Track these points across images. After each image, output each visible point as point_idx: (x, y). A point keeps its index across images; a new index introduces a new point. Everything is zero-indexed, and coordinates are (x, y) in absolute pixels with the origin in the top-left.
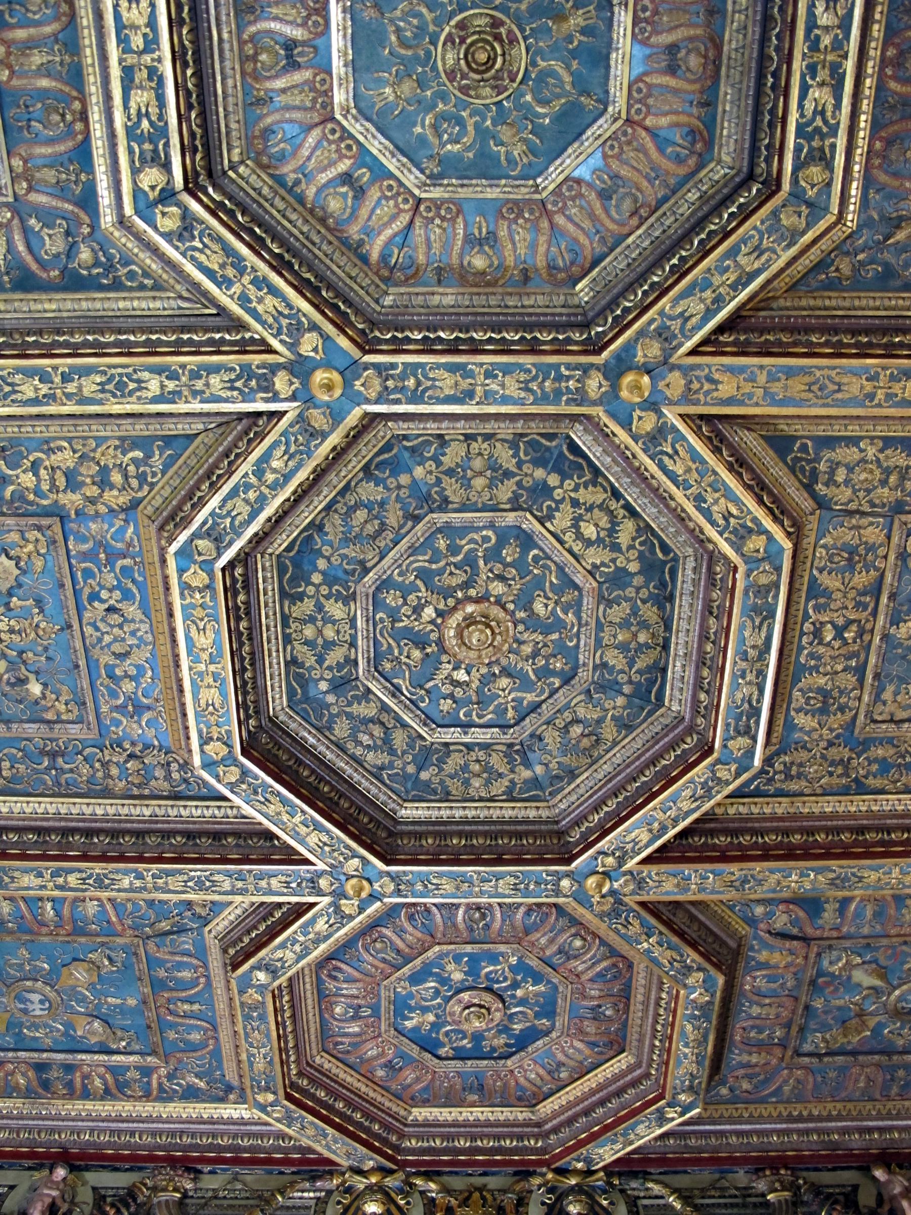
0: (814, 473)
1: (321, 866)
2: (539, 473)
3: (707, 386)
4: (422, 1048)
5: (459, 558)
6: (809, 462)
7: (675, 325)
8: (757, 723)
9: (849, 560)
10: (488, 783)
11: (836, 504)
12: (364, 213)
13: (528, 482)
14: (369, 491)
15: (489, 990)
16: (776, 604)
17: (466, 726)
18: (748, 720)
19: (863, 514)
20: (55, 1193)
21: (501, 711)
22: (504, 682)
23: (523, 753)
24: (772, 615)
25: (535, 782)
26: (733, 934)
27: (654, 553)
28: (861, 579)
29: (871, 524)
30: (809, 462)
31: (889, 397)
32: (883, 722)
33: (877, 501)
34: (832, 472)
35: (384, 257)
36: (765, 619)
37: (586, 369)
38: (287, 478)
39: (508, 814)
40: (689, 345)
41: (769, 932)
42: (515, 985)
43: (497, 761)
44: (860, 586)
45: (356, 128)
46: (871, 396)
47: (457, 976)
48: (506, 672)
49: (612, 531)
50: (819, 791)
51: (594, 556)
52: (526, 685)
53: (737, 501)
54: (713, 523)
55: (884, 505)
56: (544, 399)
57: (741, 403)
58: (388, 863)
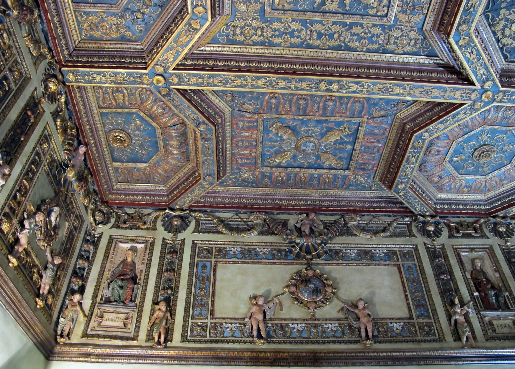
0: (422, 43)
7: (468, 112)
11: (415, 31)
16: (462, 15)
24: (465, 10)
30: (424, 48)
31: (405, 88)
33: (399, 31)
36: (468, 10)
37: (501, 101)
46: (411, 89)
53: (465, 57)
54: (477, 50)
55: (396, 29)
57: (454, 88)
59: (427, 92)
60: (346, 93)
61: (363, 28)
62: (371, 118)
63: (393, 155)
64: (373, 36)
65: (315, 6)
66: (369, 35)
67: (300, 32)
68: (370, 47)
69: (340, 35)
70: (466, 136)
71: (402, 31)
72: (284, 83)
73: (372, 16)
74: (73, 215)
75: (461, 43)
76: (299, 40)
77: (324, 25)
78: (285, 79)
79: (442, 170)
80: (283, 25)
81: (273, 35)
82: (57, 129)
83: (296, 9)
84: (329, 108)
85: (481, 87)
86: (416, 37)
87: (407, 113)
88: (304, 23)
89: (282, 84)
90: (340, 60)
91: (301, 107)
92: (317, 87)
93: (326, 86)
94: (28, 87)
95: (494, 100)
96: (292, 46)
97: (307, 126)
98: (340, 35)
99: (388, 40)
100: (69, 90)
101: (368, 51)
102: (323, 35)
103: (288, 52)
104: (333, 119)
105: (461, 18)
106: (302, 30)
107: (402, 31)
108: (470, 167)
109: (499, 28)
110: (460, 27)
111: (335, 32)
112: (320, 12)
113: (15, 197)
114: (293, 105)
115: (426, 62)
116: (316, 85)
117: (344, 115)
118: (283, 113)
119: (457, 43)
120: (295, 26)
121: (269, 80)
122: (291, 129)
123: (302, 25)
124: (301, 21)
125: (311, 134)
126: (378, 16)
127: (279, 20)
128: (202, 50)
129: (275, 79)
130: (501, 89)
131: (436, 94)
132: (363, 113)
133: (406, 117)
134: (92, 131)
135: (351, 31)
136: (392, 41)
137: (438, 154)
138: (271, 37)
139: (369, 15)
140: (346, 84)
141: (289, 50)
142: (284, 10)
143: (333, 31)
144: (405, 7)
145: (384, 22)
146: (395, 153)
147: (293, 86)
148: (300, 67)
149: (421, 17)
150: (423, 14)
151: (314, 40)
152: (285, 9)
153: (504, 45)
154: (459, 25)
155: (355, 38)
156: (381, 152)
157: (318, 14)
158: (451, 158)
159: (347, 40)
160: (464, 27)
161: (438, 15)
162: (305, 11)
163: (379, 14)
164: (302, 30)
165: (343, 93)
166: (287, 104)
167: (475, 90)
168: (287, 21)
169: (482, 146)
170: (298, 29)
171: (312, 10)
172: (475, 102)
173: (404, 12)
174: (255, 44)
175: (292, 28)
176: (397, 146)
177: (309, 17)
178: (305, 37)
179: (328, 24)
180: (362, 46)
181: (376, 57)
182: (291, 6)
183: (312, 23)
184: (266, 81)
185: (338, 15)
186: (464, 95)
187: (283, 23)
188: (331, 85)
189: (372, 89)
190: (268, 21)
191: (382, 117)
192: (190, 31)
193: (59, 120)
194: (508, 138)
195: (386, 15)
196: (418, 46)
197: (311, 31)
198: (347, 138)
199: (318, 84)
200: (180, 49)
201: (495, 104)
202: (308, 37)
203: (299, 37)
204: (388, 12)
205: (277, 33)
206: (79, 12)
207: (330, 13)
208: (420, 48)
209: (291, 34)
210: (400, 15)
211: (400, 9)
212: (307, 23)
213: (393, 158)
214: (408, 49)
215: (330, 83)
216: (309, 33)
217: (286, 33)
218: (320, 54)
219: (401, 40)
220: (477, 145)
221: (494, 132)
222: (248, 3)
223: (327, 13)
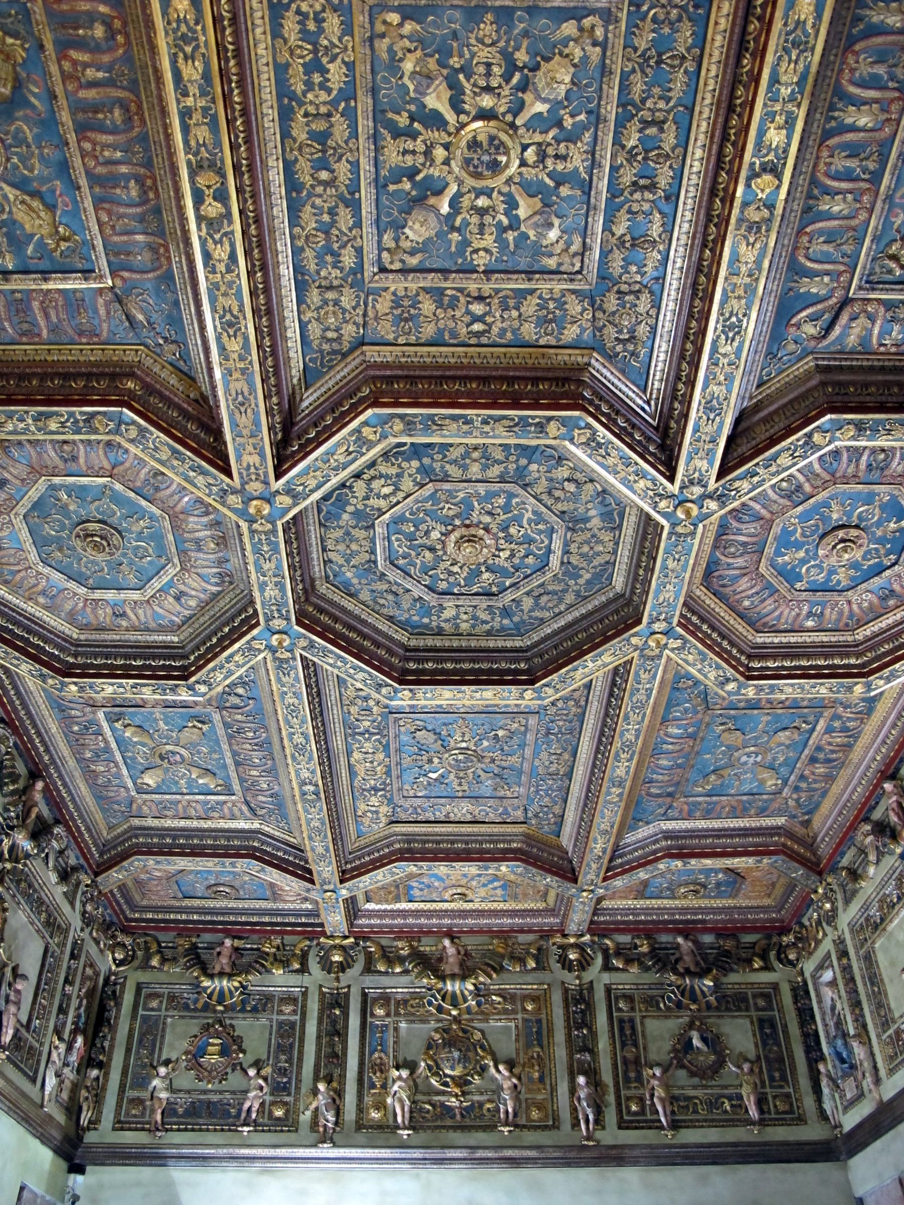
0: (334, 352)
1: (636, 654)
2: (345, 516)
3: (252, 470)
4: (877, 574)
5: (413, 553)
6: (323, 357)
8: (533, 418)
9: (406, 320)
10: (600, 542)
12: (193, 593)
13: (353, 522)
14: (365, 596)
15: (823, 536)
17: (549, 551)
18: (530, 425)
19: (365, 315)
20: (894, 798)
21: (540, 532)
22: (512, 531)
23: (577, 521)
25: (607, 516)
26: (808, 375)
27: (404, 453)
28: (427, 306)
29: (374, 307)
30: (323, 357)
32: (582, 261)
34: (329, 340)
35: (217, 584)
37: (252, 532)
38: (340, 657)
39: (630, 532)
40: (227, 480)
41: (824, 337)
42: (825, 519)
43: (580, 538)
44: (433, 307)
45: (150, 592)
46: (243, 371)
47: (802, 554)
48: (505, 529)
49: (387, 477)
50: (653, 312)
51: (407, 484)
52: (518, 520)
56: (276, 550)
58: (639, 622)
59: (242, 404)
60: (200, 237)
61: (350, 230)
62: (116, 295)
63: (34, 375)
64: (336, 255)
65: (390, 115)
66: (336, 246)
67: (323, 86)
68: (309, 253)
69: (326, 184)
70: (132, 495)
71: (354, 308)
72: (196, 77)
73: (379, 242)
75: (367, 431)
76: (299, 88)
77: (346, 142)
78: (206, 76)
79: (23, 480)
81: (305, 16)
83: (377, 69)
84: (118, 191)
85: (277, 492)
86: (346, 337)
87: (156, 369)
88: (348, 94)
89: (192, 72)
90: (268, 195)
91: (100, 116)
92: (201, 167)
93: (209, 187)
95: (251, 521)
96: (281, 70)
97: (38, 138)
98: (326, 184)
99: (330, 288)
101: (297, 252)
102: (323, 144)
103: (264, 61)
104: (88, 203)
105: (415, 416)
106: (329, 91)
107: (354, 308)
108: (52, 528)
109: (383, 468)
110: (397, 420)
111: (333, 171)
112: (375, 128)
114: (100, 90)
115: (294, 372)
116: (206, 164)
117: (108, 231)
118: (67, 65)
119: (366, 423)
120: (336, 73)
121: (195, 32)
122: (13, 93)
123: (340, 89)
124: (352, 84)
125: (16, 154)
126: (379, 255)
127: (348, 29)
129: (203, 50)
130: (279, 524)
131: (243, 420)
132: (126, 274)
133: (148, 372)
135: (341, 205)
136: (330, 295)
137: (66, 461)
138: (298, 12)
139: (380, 236)
140: (226, 234)
141: (267, 64)
142: (371, 39)
143: (335, 166)
144: (406, 303)
145: (370, 269)
146: (43, 377)
147: (190, 101)
148: (238, 107)
149: (391, 337)
150: (396, 339)
151: (307, 125)
152: (377, 43)
153: (351, 487)
154: (402, 417)
155: (326, 218)
156: (24, 339)
157: (371, 124)
158: (62, 486)
159: (318, 201)
160: (398, 426)
161: (401, 367)
162: (374, 91)
163: (385, 255)
164: (329, 91)
165: (199, 229)
166: (100, 75)
167: (266, 483)
168: (346, 49)
169: (115, 529)
170: (328, 80)
171: (379, 108)
172: (241, 491)
173: (397, 302)
175: (331, 66)
176: (66, 376)
177: (364, 103)
178: (311, 102)
179: (351, 150)
180: (307, 237)
181: (286, 272)
182: (385, 56)
183: (350, 115)
184: (192, 23)
185: (373, 170)
186: (252, 470)
187: (340, 40)
188: (215, 199)
189: (225, 295)
191: (128, 317)
194: (150, 563)
195: (383, 270)
196: (326, 347)
197: (329, 115)
198: (35, 250)
199: (212, 165)
201: (244, 526)
202: (311, 109)
203: (309, 86)
204: (392, 271)
205: (312, 26)
207: (376, 150)
208: (321, 351)
209: (315, 66)
210: (388, 296)
211: (401, 293)
212: (347, 100)
213: (29, 377)
214: (315, 330)
215: (221, 196)
216: (323, 110)
217: (315, 51)
218: (272, 145)
219: (334, 313)
220: (114, 521)
221: (157, 538)
223: (375, 144)
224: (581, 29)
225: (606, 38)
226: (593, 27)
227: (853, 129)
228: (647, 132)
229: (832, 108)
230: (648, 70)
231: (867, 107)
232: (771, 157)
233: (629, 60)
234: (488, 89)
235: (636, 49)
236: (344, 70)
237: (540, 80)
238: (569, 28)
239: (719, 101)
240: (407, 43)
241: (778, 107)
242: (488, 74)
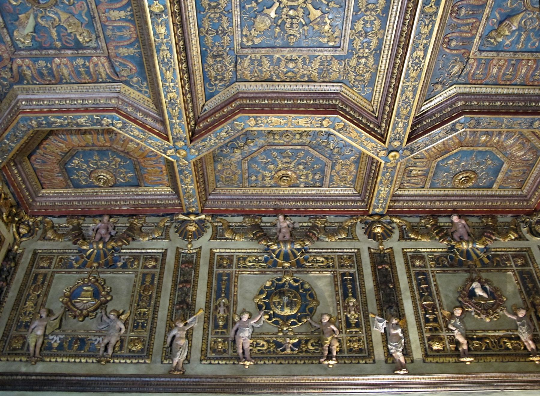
67: (367, 22)
74: (508, 260)
80: (356, 38)
82: (416, 240)
94: (362, 257)
100: (392, 212)
106: (364, 20)
113: (427, 321)
128: (376, 109)
134: (444, 201)
138: (370, 49)
174: (377, 62)
190: (352, 52)
192: (346, 130)
193: (410, 234)
200: (364, 138)
206: (329, 185)
216: (368, 13)
222: (331, 71)
224: (252, 41)
225: (242, 37)
226: (247, 42)
227: (119, 9)
228: (215, 4)
229: (132, 15)
230: (221, 28)
231: (117, 19)
232: (159, 21)
233: (230, 32)
234: (292, 18)
235: (228, 35)
236: (355, 27)
237: (268, 23)
238: (257, 41)
239: (187, 21)
240: (327, 35)
241: (165, 41)
242: (292, 24)
